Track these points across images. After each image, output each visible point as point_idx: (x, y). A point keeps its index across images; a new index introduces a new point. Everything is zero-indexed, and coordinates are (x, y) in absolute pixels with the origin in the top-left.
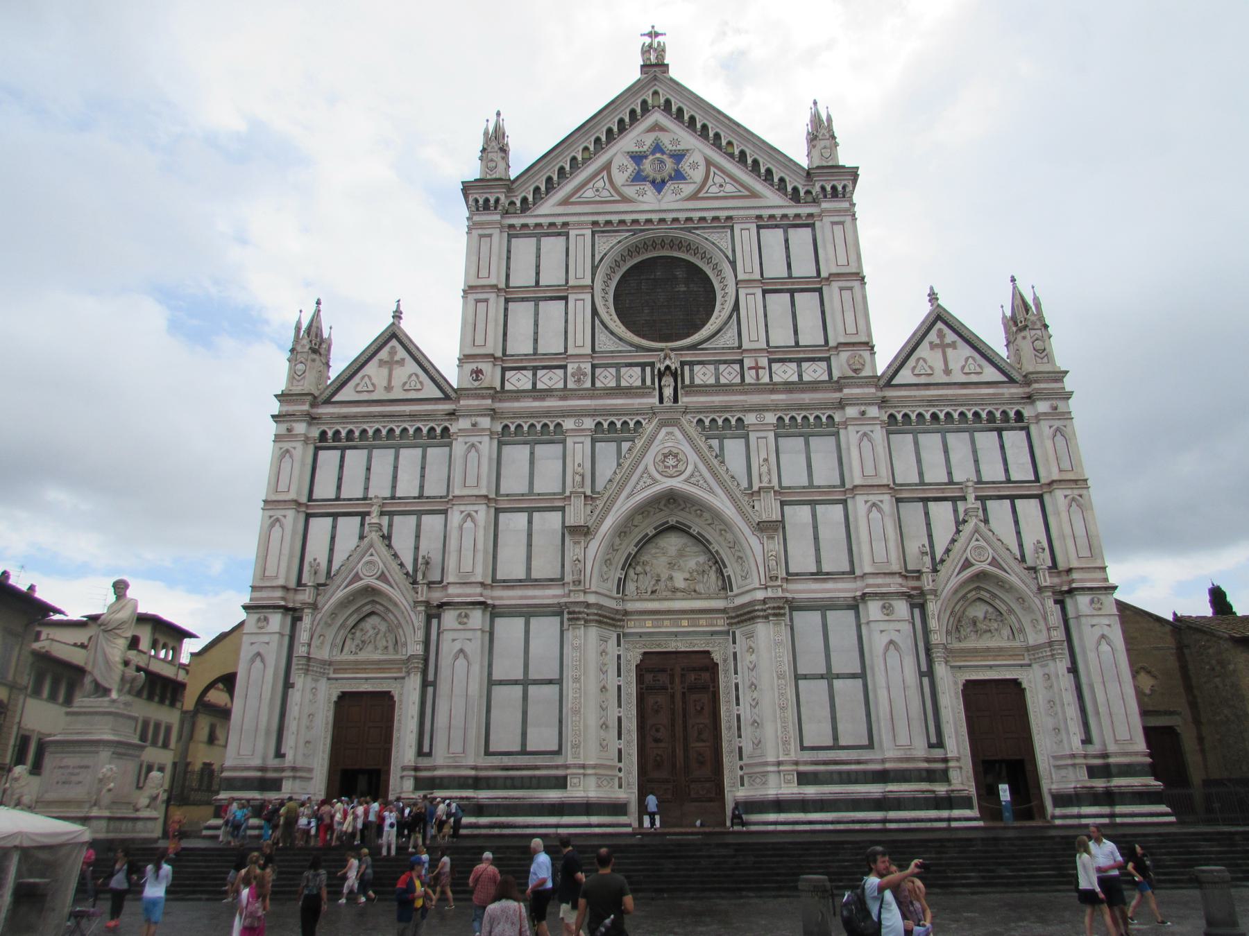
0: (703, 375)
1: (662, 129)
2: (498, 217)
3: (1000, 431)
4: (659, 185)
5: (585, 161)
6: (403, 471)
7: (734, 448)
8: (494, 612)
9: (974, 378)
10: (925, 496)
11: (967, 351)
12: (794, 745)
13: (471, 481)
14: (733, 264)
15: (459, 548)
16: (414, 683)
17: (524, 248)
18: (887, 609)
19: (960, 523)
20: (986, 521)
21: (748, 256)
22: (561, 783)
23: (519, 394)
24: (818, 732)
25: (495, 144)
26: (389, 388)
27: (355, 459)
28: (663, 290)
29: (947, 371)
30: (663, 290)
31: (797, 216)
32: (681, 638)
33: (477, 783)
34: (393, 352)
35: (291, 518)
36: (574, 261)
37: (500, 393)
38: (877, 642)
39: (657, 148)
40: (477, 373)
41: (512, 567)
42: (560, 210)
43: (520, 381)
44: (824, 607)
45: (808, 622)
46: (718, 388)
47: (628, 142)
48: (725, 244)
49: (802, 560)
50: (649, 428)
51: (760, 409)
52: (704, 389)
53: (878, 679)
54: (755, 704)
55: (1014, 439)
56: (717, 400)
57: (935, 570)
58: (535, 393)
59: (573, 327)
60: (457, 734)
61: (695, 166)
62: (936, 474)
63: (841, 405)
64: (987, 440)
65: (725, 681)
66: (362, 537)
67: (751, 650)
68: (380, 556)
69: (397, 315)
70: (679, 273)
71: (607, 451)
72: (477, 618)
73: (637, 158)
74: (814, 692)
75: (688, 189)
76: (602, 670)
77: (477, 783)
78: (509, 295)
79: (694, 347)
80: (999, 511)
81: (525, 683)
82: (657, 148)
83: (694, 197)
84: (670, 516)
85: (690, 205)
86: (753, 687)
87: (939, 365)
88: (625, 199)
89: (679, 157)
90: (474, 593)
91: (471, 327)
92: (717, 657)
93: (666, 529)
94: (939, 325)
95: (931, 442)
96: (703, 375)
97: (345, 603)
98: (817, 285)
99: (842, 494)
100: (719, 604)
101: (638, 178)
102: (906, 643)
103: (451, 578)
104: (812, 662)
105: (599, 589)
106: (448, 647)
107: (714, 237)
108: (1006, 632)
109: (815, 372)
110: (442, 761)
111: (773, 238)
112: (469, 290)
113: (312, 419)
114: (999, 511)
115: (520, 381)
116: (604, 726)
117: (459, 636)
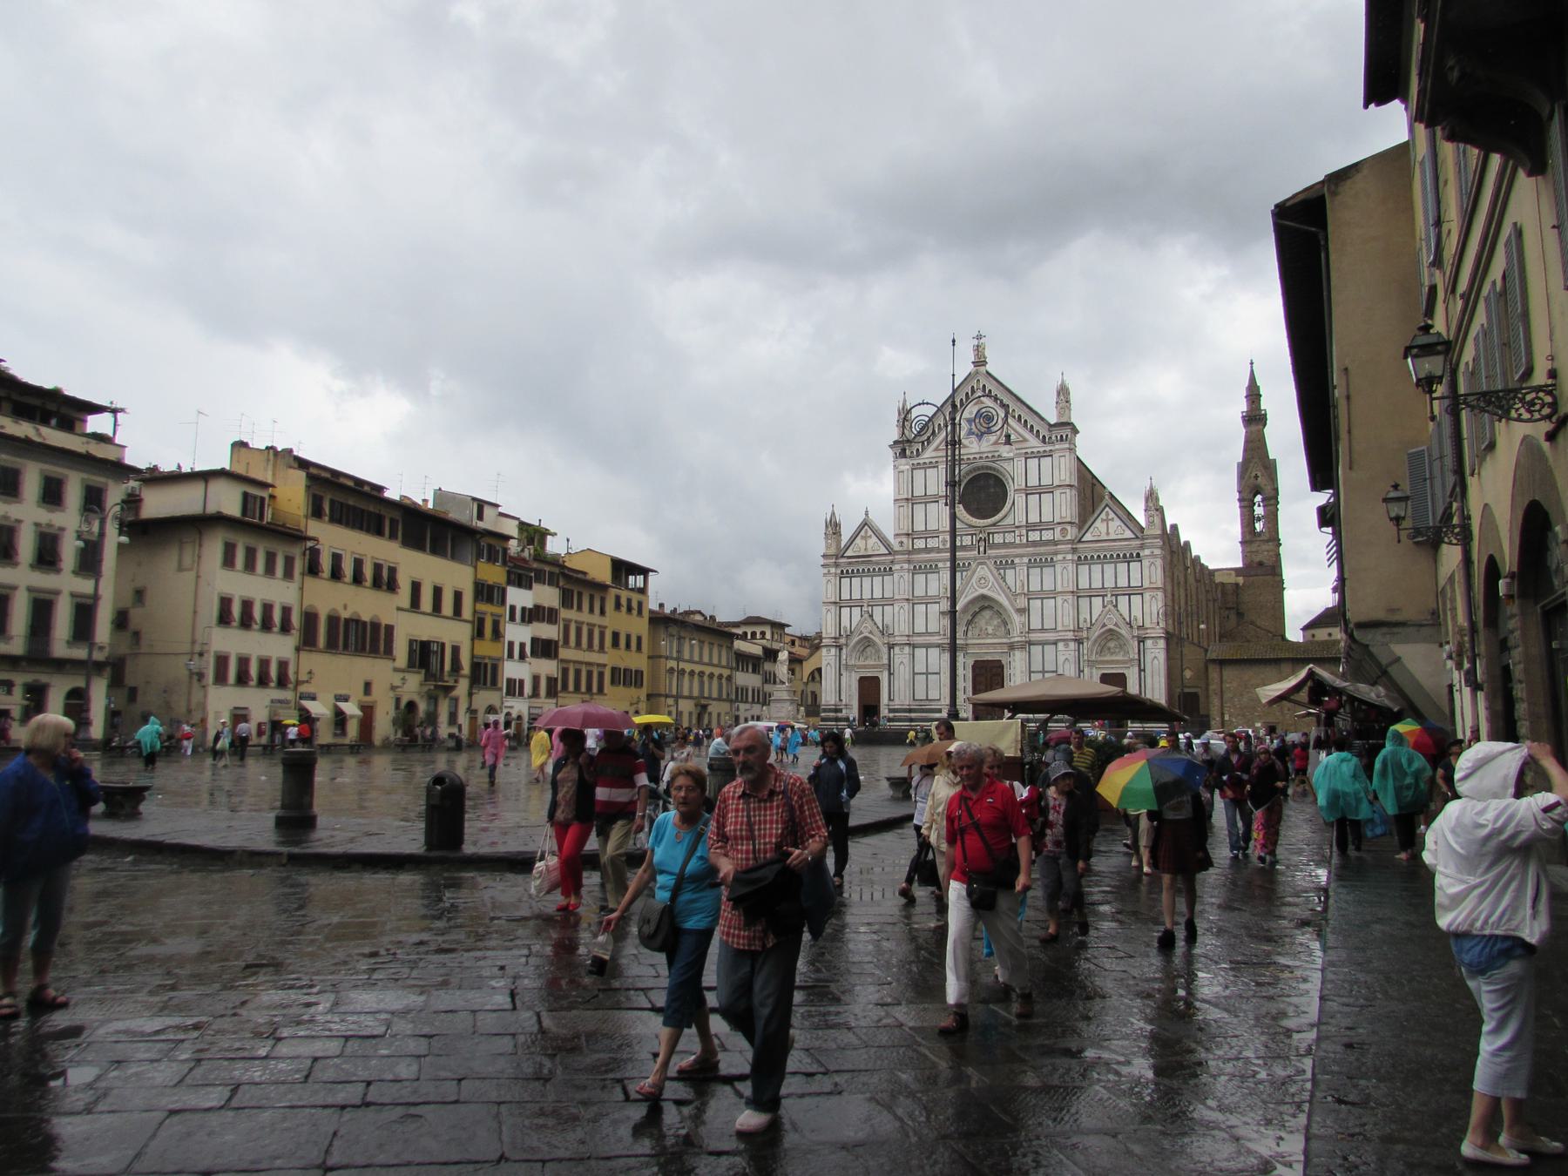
0: (998, 539)
6: (873, 587)
7: (1010, 573)
8: (914, 646)
10: (1091, 594)
15: (898, 619)
16: (886, 674)
17: (919, 474)
18: (1067, 646)
21: (1017, 473)
23: (920, 551)
25: (905, 416)
27: (856, 581)
28: (981, 492)
30: (981, 492)
32: (990, 655)
33: (910, 711)
37: (914, 551)
38: (1061, 659)
41: (920, 628)
44: (1043, 643)
45: (1036, 650)
46: (1005, 545)
48: (1010, 469)
49: (1036, 624)
50: (973, 565)
51: (1021, 556)
52: (998, 546)
55: (1135, 566)
56: (1003, 552)
58: (927, 550)
62: (1097, 584)
63: (1056, 554)
64: (1122, 567)
68: (869, 624)
72: (907, 649)
77: (910, 711)
80: (1123, 600)
81: (927, 674)
87: (1104, 530)
90: (904, 640)
93: (982, 609)
95: (1097, 568)
97: (858, 642)
99: (1053, 594)
102: (1072, 659)
106: (897, 661)
107: (1005, 465)
110: (897, 704)
111: (1033, 463)
113: (837, 565)
114: (1123, 600)
115: (920, 544)
117: (901, 657)
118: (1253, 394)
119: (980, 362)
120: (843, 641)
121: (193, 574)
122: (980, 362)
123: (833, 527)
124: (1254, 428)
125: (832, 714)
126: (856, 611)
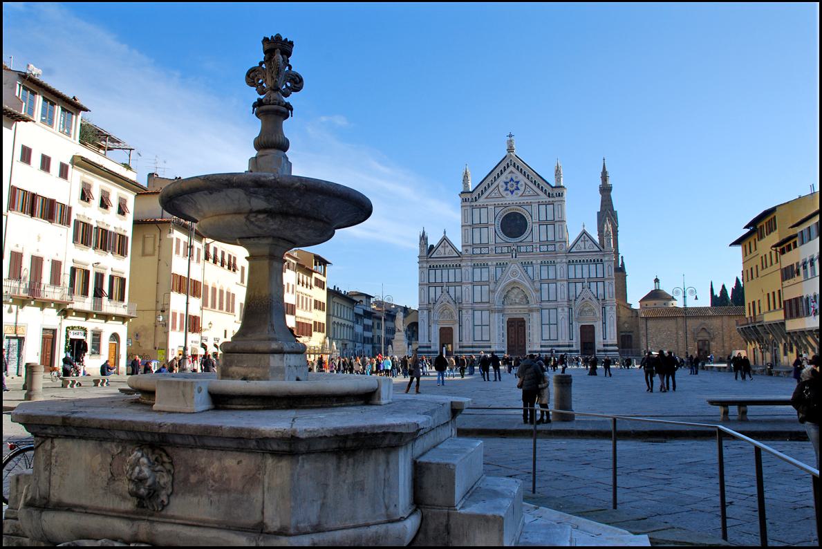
0: (523, 249)
1: (513, 173)
2: (468, 204)
3: (596, 264)
4: (512, 192)
5: (492, 184)
9: (592, 250)
11: (590, 242)
12: (540, 339)
13: (467, 279)
14: (531, 216)
18: (563, 310)
19: (583, 288)
20: (589, 288)
21: (534, 215)
22: (490, 347)
24: (546, 336)
26: (445, 254)
27: (438, 272)
28: (514, 225)
29: (585, 248)
30: (514, 225)
31: (549, 201)
33: (472, 347)
34: (445, 244)
35: (426, 288)
36: (490, 216)
38: (560, 317)
39: (512, 180)
40: (467, 250)
41: (477, 299)
42: (485, 200)
43: (477, 251)
47: (503, 178)
48: (530, 211)
49: (545, 297)
50: (510, 265)
53: (559, 325)
54: (533, 330)
57: (575, 300)
59: (491, 235)
60: (467, 337)
61: (522, 185)
64: (593, 267)
65: (527, 325)
66: (442, 292)
67: (533, 318)
69: (445, 232)
70: (518, 217)
71: (499, 270)
73: (506, 183)
74: (546, 328)
75: (520, 193)
76: (499, 322)
77: (472, 347)
78: (473, 226)
79: (521, 242)
80: (593, 285)
81: (482, 326)
82: (512, 180)
83: (521, 196)
84: (514, 286)
85: (521, 198)
86: (533, 326)
87: (583, 247)
88: (503, 197)
89: (517, 182)
91: (464, 237)
92: (525, 319)
94: (584, 235)
96: (523, 249)
98: (553, 223)
99: (555, 281)
100: (526, 306)
101: (506, 189)
102: (566, 317)
103: (464, 302)
104: (546, 321)
105: (498, 305)
106: (464, 319)
107: (526, 207)
108: (592, 314)
109: (551, 248)
110: (465, 343)
111: (543, 208)
112: (462, 226)
115: (477, 251)
116: (499, 335)
117: (466, 316)
118: (604, 176)
119: (510, 149)
120: (431, 306)
121: (156, 258)
122: (510, 149)
123: (423, 238)
124: (605, 194)
125: (426, 350)
126: (439, 289)
